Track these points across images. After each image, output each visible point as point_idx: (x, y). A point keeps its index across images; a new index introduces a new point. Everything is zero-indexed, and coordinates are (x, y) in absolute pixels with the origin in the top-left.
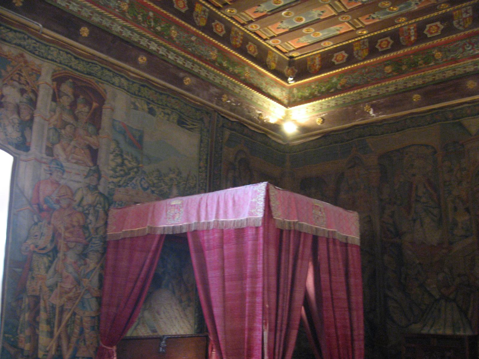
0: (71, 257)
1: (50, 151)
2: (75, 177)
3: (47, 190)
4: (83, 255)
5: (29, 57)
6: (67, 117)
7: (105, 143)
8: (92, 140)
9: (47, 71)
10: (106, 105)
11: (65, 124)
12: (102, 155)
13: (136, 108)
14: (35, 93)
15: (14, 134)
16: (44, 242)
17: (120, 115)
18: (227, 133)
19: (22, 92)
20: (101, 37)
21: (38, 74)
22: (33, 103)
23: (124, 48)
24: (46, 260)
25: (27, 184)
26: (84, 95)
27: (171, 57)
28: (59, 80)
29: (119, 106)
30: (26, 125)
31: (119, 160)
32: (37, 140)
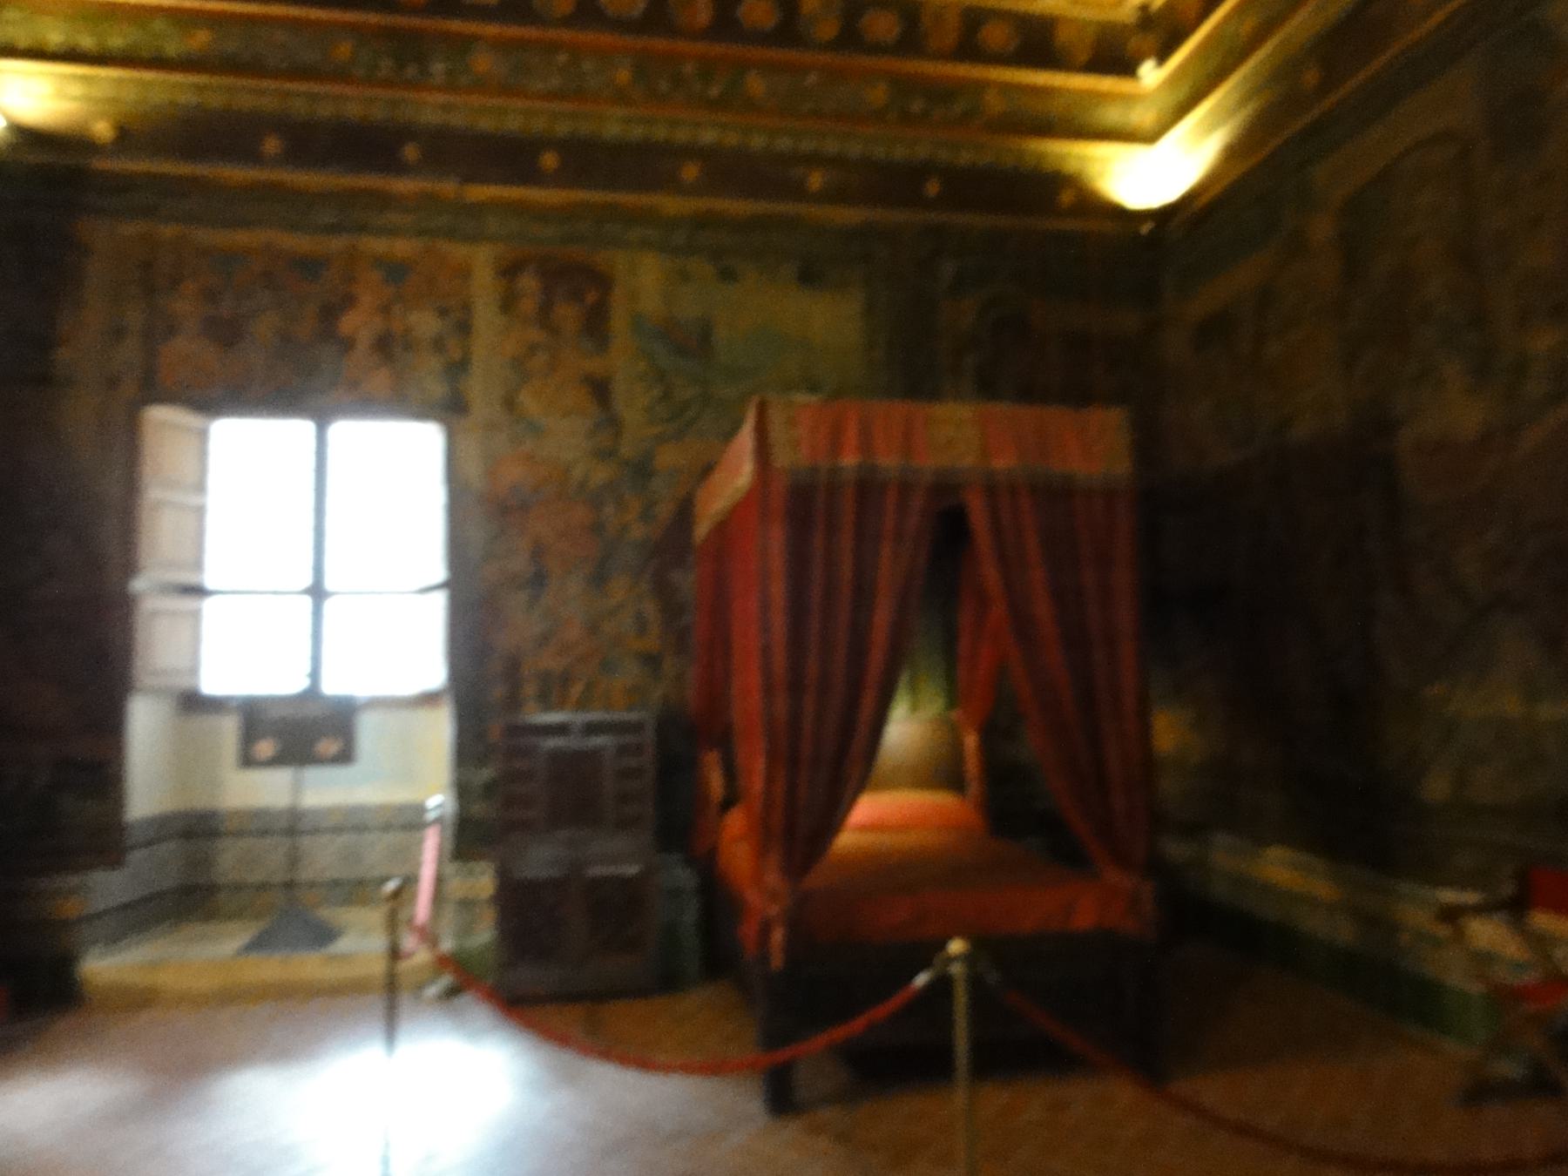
0: (575, 585)
1: (510, 403)
2: (567, 438)
3: (514, 473)
4: (599, 579)
5: (444, 246)
6: (535, 335)
7: (622, 362)
8: (594, 365)
9: (482, 260)
10: (618, 294)
11: (532, 349)
12: (619, 389)
13: (685, 277)
14: (467, 307)
15: (438, 389)
16: (520, 564)
17: (651, 302)
18: (948, 268)
19: (443, 312)
20: (588, 160)
21: (464, 273)
22: (464, 328)
23: (642, 164)
24: (523, 596)
25: (473, 471)
26: (568, 285)
27: (758, 142)
28: (509, 271)
29: (645, 282)
30: (458, 368)
31: (656, 392)
32: (481, 388)
